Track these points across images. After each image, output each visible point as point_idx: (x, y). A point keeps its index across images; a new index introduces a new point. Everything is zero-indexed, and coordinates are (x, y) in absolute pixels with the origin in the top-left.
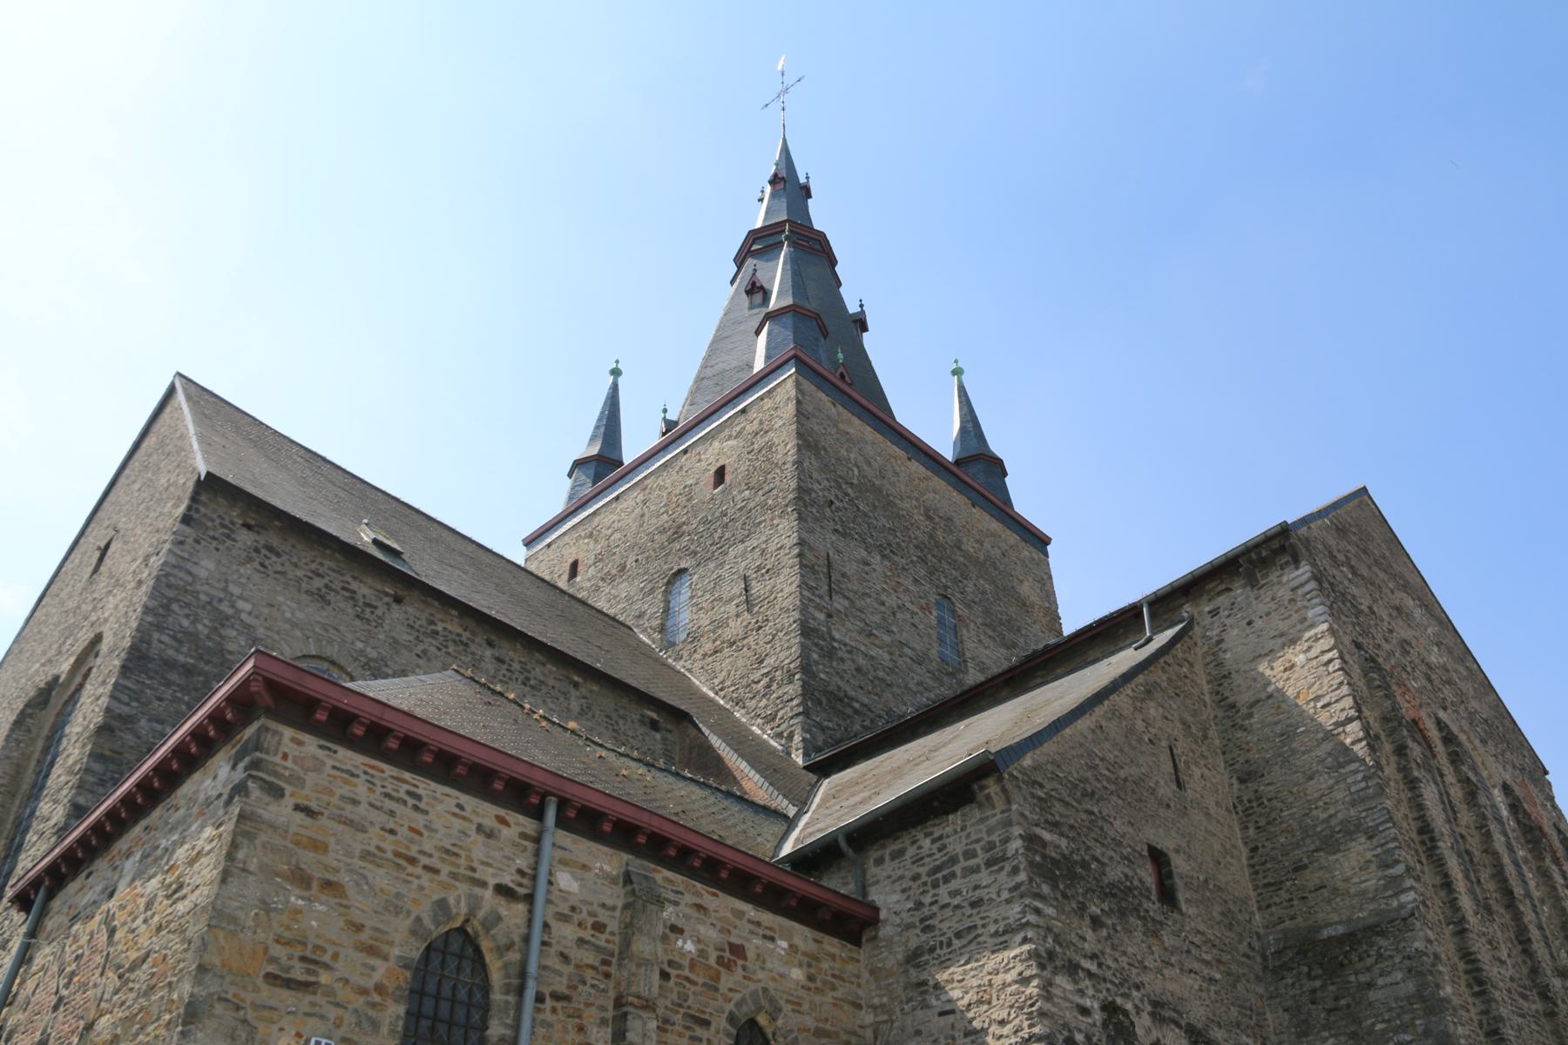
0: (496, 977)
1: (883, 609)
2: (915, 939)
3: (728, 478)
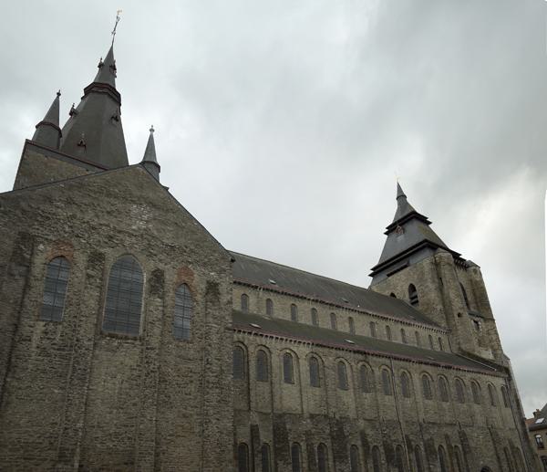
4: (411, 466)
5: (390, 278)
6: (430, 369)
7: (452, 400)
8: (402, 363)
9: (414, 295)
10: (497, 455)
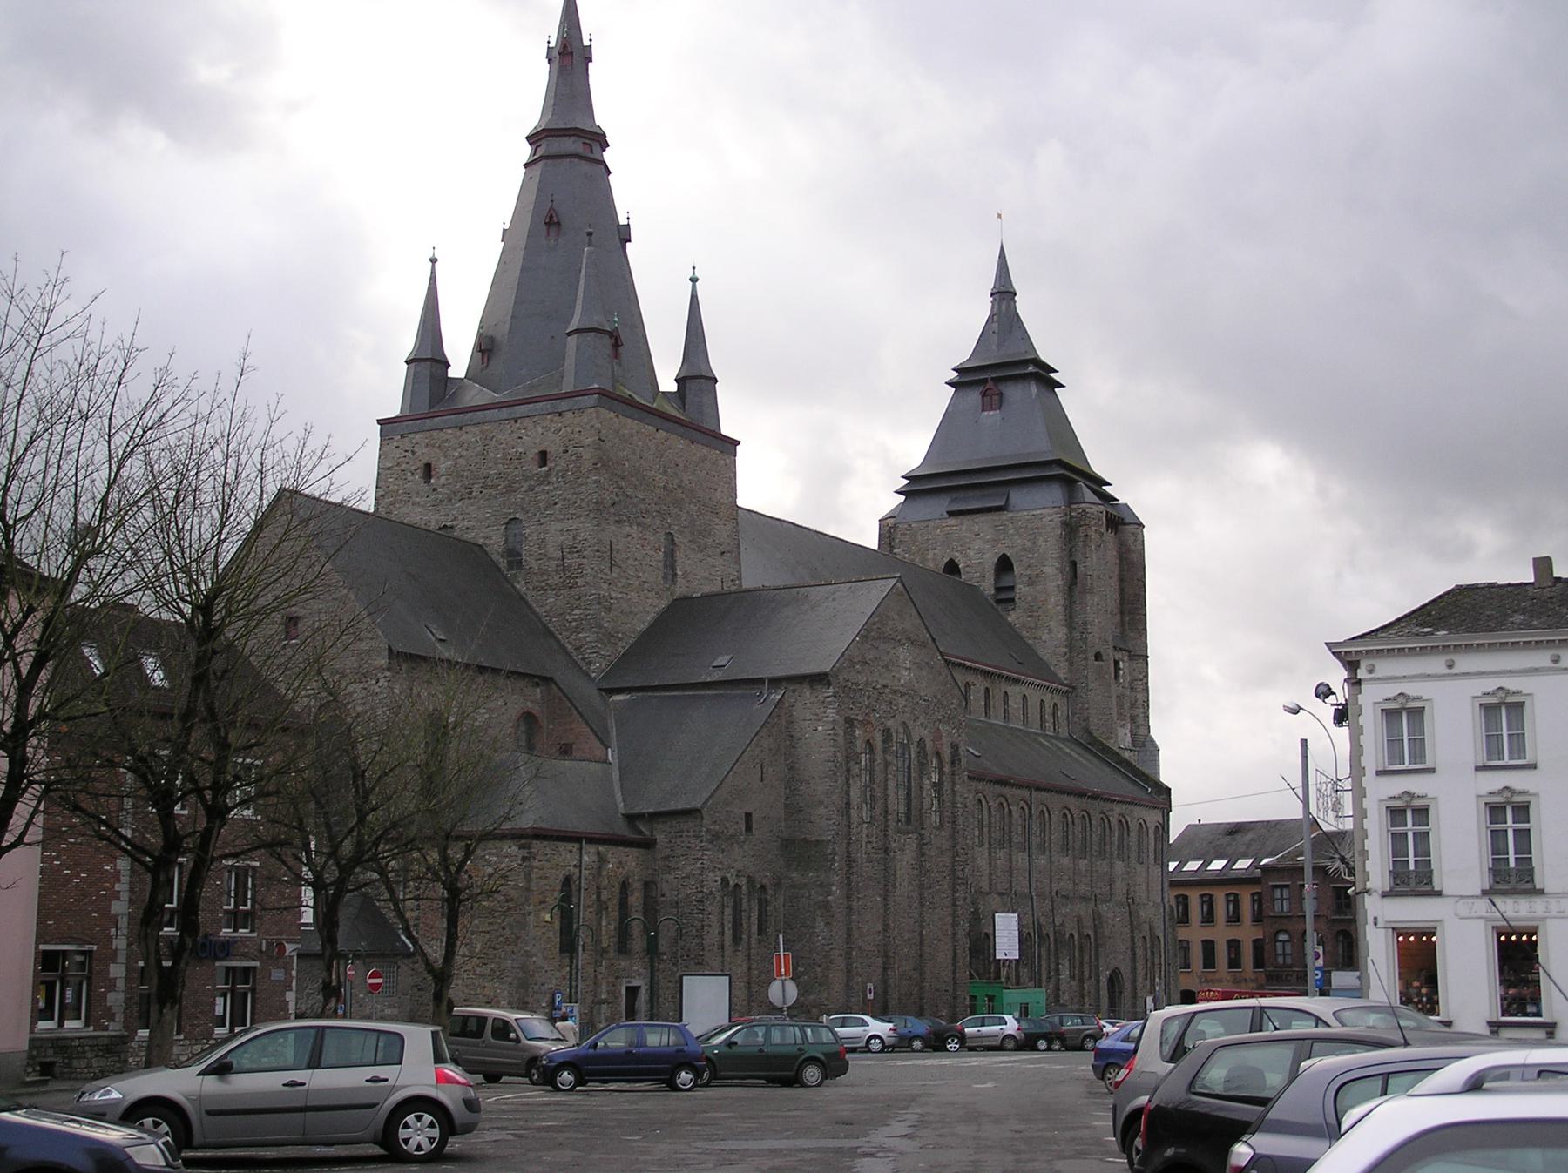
0: (573, 887)
1: (636, 563)
2: (668, 852)
3: (550, 465)
4: (1040, 966)
5: (952, 521)
6: (1072, 802)
7: (1092, 855)
8: (1044, 795)
9: (1006, 582)
10: (1133, 949)
